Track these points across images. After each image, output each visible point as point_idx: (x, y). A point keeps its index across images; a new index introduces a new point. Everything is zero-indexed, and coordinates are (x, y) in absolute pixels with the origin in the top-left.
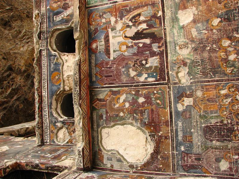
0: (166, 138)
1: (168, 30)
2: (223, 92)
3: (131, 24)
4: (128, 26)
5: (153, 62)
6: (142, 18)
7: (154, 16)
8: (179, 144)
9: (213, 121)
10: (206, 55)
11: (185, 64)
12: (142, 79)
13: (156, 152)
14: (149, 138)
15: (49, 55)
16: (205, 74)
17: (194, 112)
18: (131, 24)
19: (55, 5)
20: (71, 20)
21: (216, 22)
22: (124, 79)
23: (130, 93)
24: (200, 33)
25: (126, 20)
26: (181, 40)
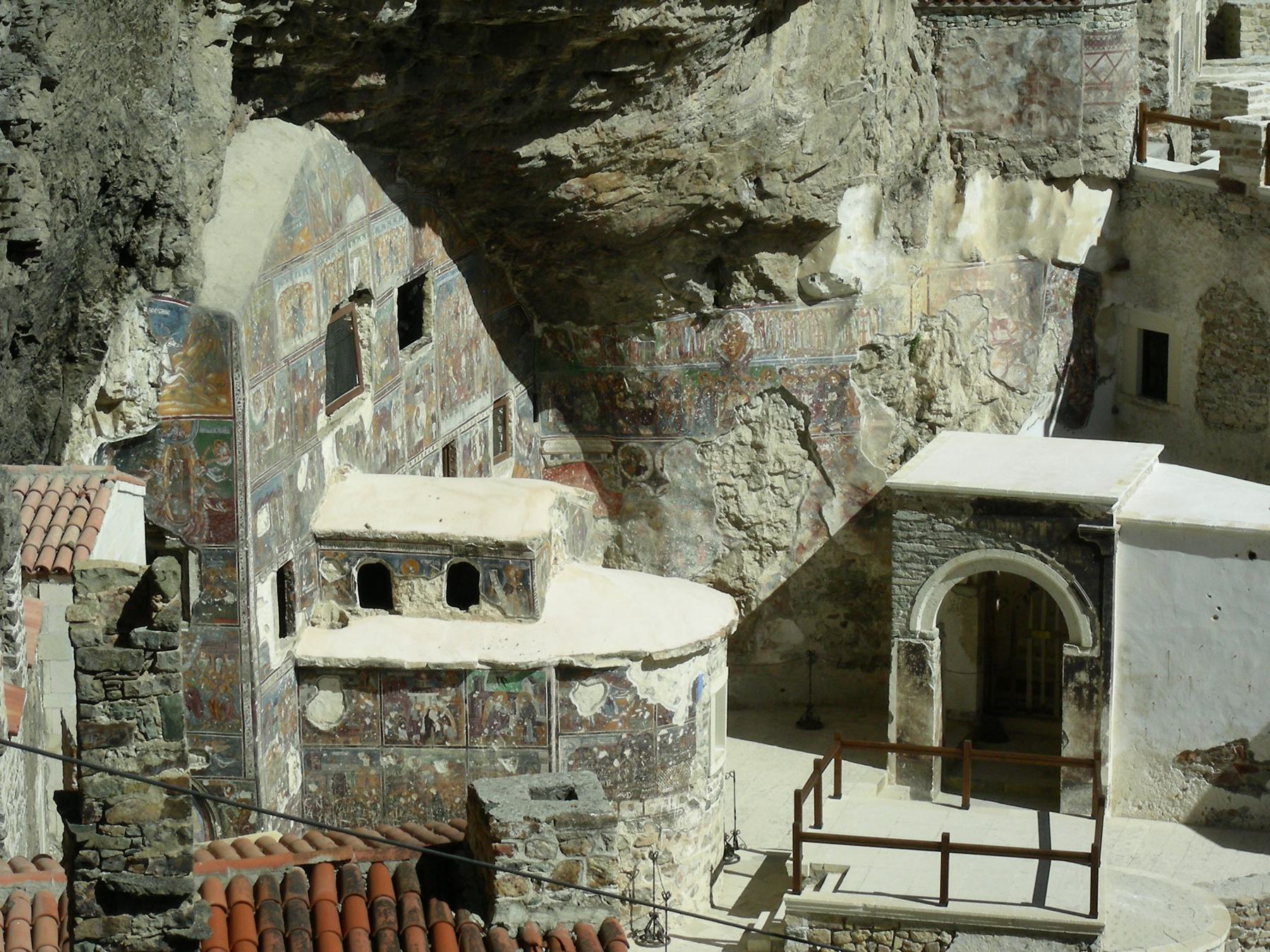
0: (333, 741)
1: (431, 750)
2: (374, 791)
3: (441, 716)
4: (439, 713)
5: (403, 734)
6: (446, 727)
7: (446, 739)
8: (328, 752)
9: (349, 782)
10: (406, 780)
11: (398, 762)
12: (387, 723)
13: (320, 732)
14: (332, 726)
15: (442, 559)
16: (389, 778)
17: (356, 767)
18: (441, 716)
19: (512, 573)
20: (488, 596)
21: (433, 791)
22: (388, 705)
23: (374, 710)
24: (425, 777)
25: (446, 712)
26: (420, 761)
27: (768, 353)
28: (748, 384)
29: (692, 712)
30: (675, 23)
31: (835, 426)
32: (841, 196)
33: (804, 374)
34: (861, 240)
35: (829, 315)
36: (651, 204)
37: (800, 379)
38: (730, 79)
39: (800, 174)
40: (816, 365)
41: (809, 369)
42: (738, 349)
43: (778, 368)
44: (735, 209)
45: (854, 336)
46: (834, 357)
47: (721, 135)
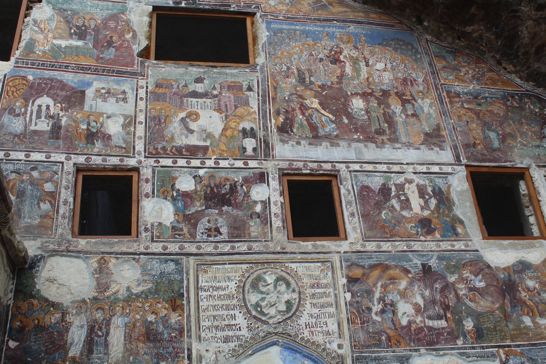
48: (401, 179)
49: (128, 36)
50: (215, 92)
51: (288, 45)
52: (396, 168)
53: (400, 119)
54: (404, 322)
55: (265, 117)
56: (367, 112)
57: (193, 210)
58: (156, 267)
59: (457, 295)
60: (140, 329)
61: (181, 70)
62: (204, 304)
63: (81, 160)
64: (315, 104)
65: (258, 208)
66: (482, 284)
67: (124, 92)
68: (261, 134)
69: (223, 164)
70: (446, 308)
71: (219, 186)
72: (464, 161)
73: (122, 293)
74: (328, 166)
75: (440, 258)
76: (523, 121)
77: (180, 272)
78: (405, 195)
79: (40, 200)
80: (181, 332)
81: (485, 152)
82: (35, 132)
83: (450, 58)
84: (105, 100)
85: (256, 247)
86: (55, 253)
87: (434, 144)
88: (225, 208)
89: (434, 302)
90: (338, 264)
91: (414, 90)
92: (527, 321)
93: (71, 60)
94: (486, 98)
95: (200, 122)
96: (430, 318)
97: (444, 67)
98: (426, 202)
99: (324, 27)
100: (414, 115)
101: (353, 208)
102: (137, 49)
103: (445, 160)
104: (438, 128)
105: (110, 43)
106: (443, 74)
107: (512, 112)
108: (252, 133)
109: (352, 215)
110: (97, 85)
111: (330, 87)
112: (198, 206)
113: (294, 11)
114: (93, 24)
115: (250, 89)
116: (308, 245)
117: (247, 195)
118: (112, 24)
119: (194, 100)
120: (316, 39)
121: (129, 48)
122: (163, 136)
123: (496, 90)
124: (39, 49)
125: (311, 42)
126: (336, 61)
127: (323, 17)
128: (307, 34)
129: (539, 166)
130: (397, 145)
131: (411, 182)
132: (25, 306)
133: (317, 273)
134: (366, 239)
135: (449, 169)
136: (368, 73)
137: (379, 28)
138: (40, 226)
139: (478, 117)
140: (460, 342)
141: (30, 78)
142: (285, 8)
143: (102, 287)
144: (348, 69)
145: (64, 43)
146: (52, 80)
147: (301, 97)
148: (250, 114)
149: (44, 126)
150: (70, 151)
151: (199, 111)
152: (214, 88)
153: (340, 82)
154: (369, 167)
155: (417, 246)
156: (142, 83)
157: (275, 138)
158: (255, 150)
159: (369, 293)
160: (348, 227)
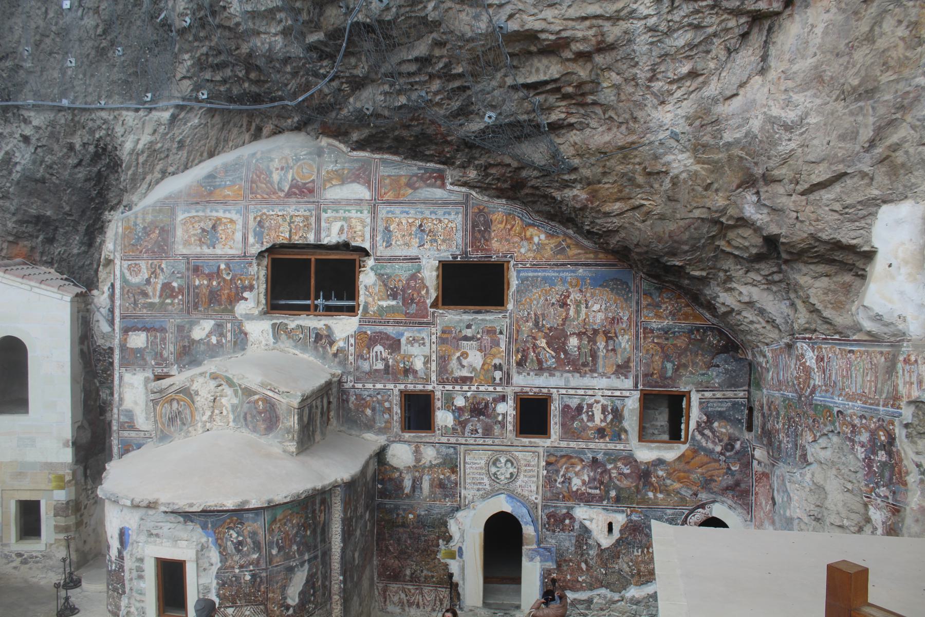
27: (827, 391)
28: (814, 421)
29: (121, 557)
30: (538, 26)
31: (883, 491)
32: (874, 214)
33: (857, 421)
34: (904, 270)
35: (883, 359)
36: (662, 217)
37: (854, 426)
38: (712, 89)
39: (806, 186)
40: (866, 414)
41: (862, 417)
42: (804, 382)
43: (836, 409)
44: (742, 222)
45: (901, 388)
46: (881, 408)
47: (703, 146)
48: (592, 401)
49: (423, 292)
50: (479, 336)
51: (531, 291)
52: (590, 392)
53: (601, 354)
54: (574, 489)
55: (509, 354)
56: (579, 348)
57: (463, 418)
58: (444, 450)
59: (610, 477)
60: (436, 482)
61: (458, 317)
62: (468, 471)
63: (402, 387)
64: (542, 343)
65: (500, 418)
66: (628, 471)
67: (423, 339)
68: (505, 368)
69: (482, 388)
70: (601, 483)
71: (479, 403)
72: (640, 387)
73: (428, 464)
74: (545, 391)
75: (605, 454)
76: (700, 352)
77: (456, 454)
78: (592, 411)
79: (384, 413)
80: (456, 484)
81: (659, 380)
82: (376, 370)
83: (656, 294)
84: (412, 346)
85: (496, 440)
86: (394, 442)
87: (622, 374)
88: (481, 417)
89: (595, 479)
90: (542, 454)
91: (617, 328)
92: (651, 495)
93: (391, 317)
94: (674, 333)
95: (469, 359)
96: (590, 488)
97: (648, 305)
98: (605, 417)
99: (559, 272)
100: (614, 350)
101: (557, 420)
102: (429, 302)
103: (626, 387)
104: (628, 361)
105: (412, 300)
106: (645, 312)
107: (693, 345)
108: (498, 367)
109: (556, 423)
110: (407, 334)
111: (556, 329)
112: (466, 416)
113: (539, 256)
114: (400, 284)
115: (501, 333)
116: (526, 441)
117: (494, 409)
118: (412, 283)
119: (465, 342)
120: (552, 284)
121: (424, 302)
122: (447, 370)
123: (685, 324)
124: (372, 309)
125: (548, 288)
126: (564, 305)
127: (561, 261)
128: (545, 279)
129: (698, 391)
130: (596, 375)
131: (598, 402)
132: (383, 469)
133: (529, 458)
134: (562, 439)
135: (627, 393)
136: (587, 314)
137: (603, 269)
138: (385, 428)
139: (663, 351)
140: (605, 503)
141: (369, 332)
142: (532, 255)
143: (418, 460)
144: (572, 313)
145: (384, 304)
146: (380, 333)
147: (535, 338)
148: (500, 353)
149: (380, 366)
150: (396, 381)
151: (469, 352)
152: (478, 333)
153: (563, 325)
154: (572, 392)
155: (592, 445)
156: (434, 330)
157: (514, 371)
158: (501, 379)
159: (558, 471)
160: (552, 431)
